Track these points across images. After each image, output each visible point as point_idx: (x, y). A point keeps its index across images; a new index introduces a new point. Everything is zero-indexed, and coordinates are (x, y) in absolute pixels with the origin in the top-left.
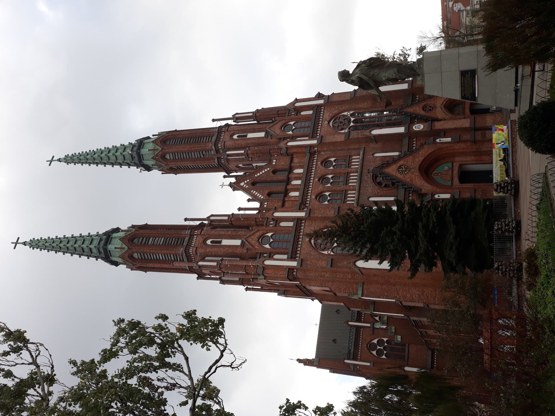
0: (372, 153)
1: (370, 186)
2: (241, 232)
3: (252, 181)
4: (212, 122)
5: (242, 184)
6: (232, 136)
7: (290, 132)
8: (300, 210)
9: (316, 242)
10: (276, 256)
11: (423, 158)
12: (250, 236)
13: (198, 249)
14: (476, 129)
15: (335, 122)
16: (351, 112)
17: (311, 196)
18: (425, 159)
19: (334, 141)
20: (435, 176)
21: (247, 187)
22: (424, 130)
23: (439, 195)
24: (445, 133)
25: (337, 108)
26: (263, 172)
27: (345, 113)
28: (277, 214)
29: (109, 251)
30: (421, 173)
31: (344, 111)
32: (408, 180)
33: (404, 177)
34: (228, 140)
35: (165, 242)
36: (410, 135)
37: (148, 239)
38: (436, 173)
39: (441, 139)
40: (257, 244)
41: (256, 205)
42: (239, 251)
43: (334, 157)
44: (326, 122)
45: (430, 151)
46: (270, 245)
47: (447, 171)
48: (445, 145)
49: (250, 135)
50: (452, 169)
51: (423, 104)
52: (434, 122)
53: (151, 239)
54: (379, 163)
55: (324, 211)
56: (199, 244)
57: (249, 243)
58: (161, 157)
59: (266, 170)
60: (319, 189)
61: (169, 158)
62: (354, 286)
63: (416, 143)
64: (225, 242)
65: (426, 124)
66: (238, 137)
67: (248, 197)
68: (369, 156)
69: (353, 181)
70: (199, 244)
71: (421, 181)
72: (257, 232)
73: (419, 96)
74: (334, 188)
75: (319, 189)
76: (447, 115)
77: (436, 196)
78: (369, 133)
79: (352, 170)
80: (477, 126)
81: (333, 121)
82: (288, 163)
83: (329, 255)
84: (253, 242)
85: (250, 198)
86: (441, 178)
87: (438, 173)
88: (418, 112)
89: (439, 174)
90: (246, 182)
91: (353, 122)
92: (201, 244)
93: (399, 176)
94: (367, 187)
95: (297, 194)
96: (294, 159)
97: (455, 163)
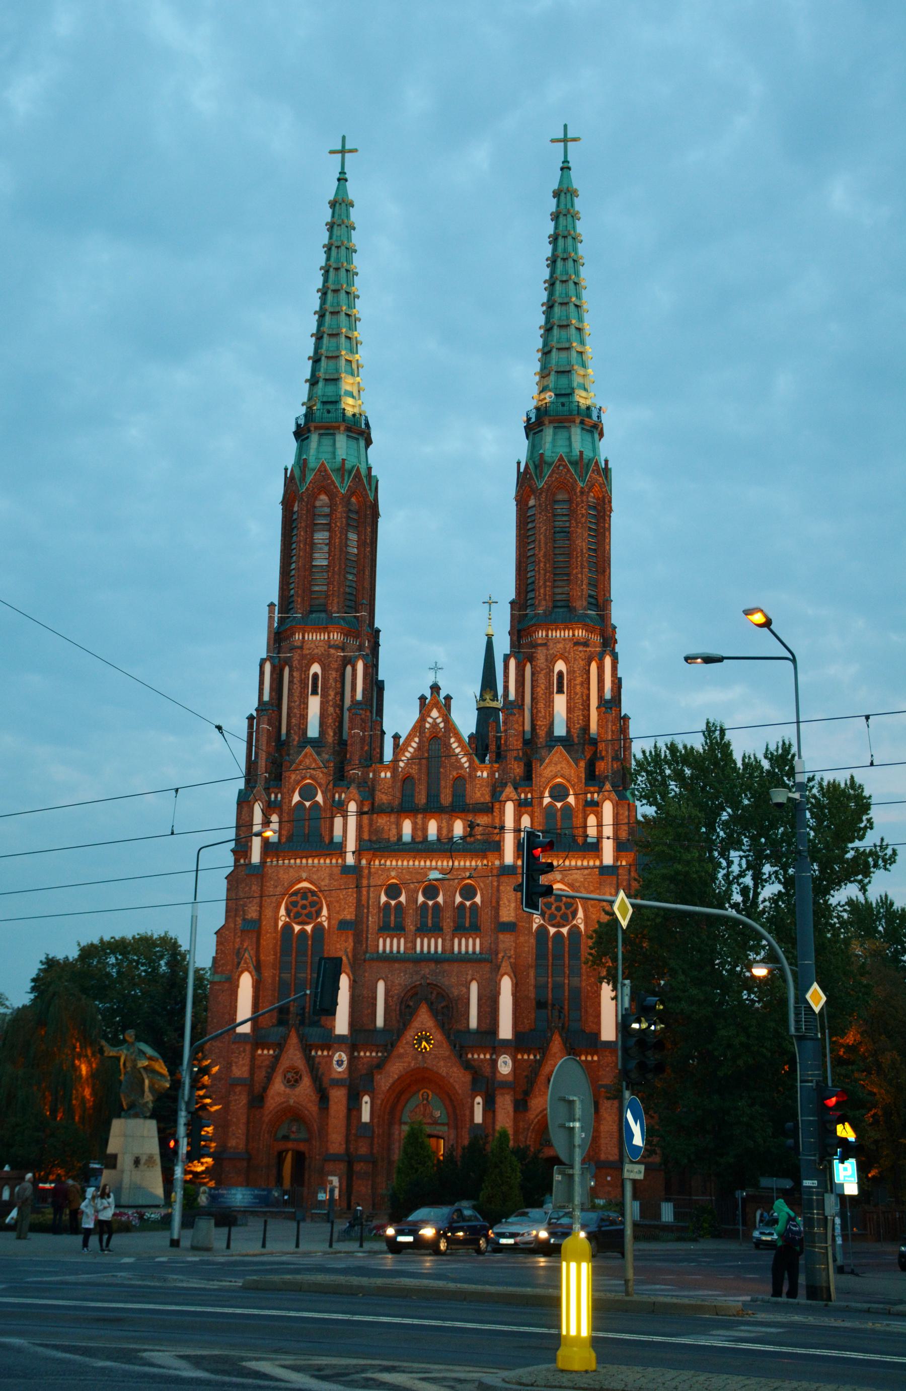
0: (478, 979)
1: (403, 979)
4: (419, 695)
5: (435, 713)
7: (547, 800)
11: (444, 1074)
13: (299, 652)
16: (582, 927)
19: (501, 902)
20: (423, 1095)
21: (427, 726)
22: (498, 1075)
23: (369, 1102)
27: (580, 914)
29: (307, 438)
31: (585, 911)
32: (402, 1051)
33: (407, 1043)
38: (428, 1096)
39: (481, 1106)
43: (482, 902)
45: (457, 1087)
46: (298, 803)
47: (432, 1116)
48: (468, 1113)
50: (435, 1123)
52: (512, 1093)
55: (350, 902)
56: (309, 649)
59: (464, 760)
62: (228, 967)
64: (314, 704)
65: (511, 1078)
67: (404, 735)
68: (470, 972)
70: (309, 649)
71: (397, 1072)
73: (595, 1061)
74: (411, 911)
76: (537, 1116)
77: (366, 1098)
78: (503, 971)
79: (448, 944)
83: (276, 919)
85: (402, 741)
86: (417, 1106)
87: (427, 1099)
88: (549, 1062)
89: (425, 1102)
91: (559, 934)
92: (310, 654)
94: (404, 975)
97: (446, 1128)
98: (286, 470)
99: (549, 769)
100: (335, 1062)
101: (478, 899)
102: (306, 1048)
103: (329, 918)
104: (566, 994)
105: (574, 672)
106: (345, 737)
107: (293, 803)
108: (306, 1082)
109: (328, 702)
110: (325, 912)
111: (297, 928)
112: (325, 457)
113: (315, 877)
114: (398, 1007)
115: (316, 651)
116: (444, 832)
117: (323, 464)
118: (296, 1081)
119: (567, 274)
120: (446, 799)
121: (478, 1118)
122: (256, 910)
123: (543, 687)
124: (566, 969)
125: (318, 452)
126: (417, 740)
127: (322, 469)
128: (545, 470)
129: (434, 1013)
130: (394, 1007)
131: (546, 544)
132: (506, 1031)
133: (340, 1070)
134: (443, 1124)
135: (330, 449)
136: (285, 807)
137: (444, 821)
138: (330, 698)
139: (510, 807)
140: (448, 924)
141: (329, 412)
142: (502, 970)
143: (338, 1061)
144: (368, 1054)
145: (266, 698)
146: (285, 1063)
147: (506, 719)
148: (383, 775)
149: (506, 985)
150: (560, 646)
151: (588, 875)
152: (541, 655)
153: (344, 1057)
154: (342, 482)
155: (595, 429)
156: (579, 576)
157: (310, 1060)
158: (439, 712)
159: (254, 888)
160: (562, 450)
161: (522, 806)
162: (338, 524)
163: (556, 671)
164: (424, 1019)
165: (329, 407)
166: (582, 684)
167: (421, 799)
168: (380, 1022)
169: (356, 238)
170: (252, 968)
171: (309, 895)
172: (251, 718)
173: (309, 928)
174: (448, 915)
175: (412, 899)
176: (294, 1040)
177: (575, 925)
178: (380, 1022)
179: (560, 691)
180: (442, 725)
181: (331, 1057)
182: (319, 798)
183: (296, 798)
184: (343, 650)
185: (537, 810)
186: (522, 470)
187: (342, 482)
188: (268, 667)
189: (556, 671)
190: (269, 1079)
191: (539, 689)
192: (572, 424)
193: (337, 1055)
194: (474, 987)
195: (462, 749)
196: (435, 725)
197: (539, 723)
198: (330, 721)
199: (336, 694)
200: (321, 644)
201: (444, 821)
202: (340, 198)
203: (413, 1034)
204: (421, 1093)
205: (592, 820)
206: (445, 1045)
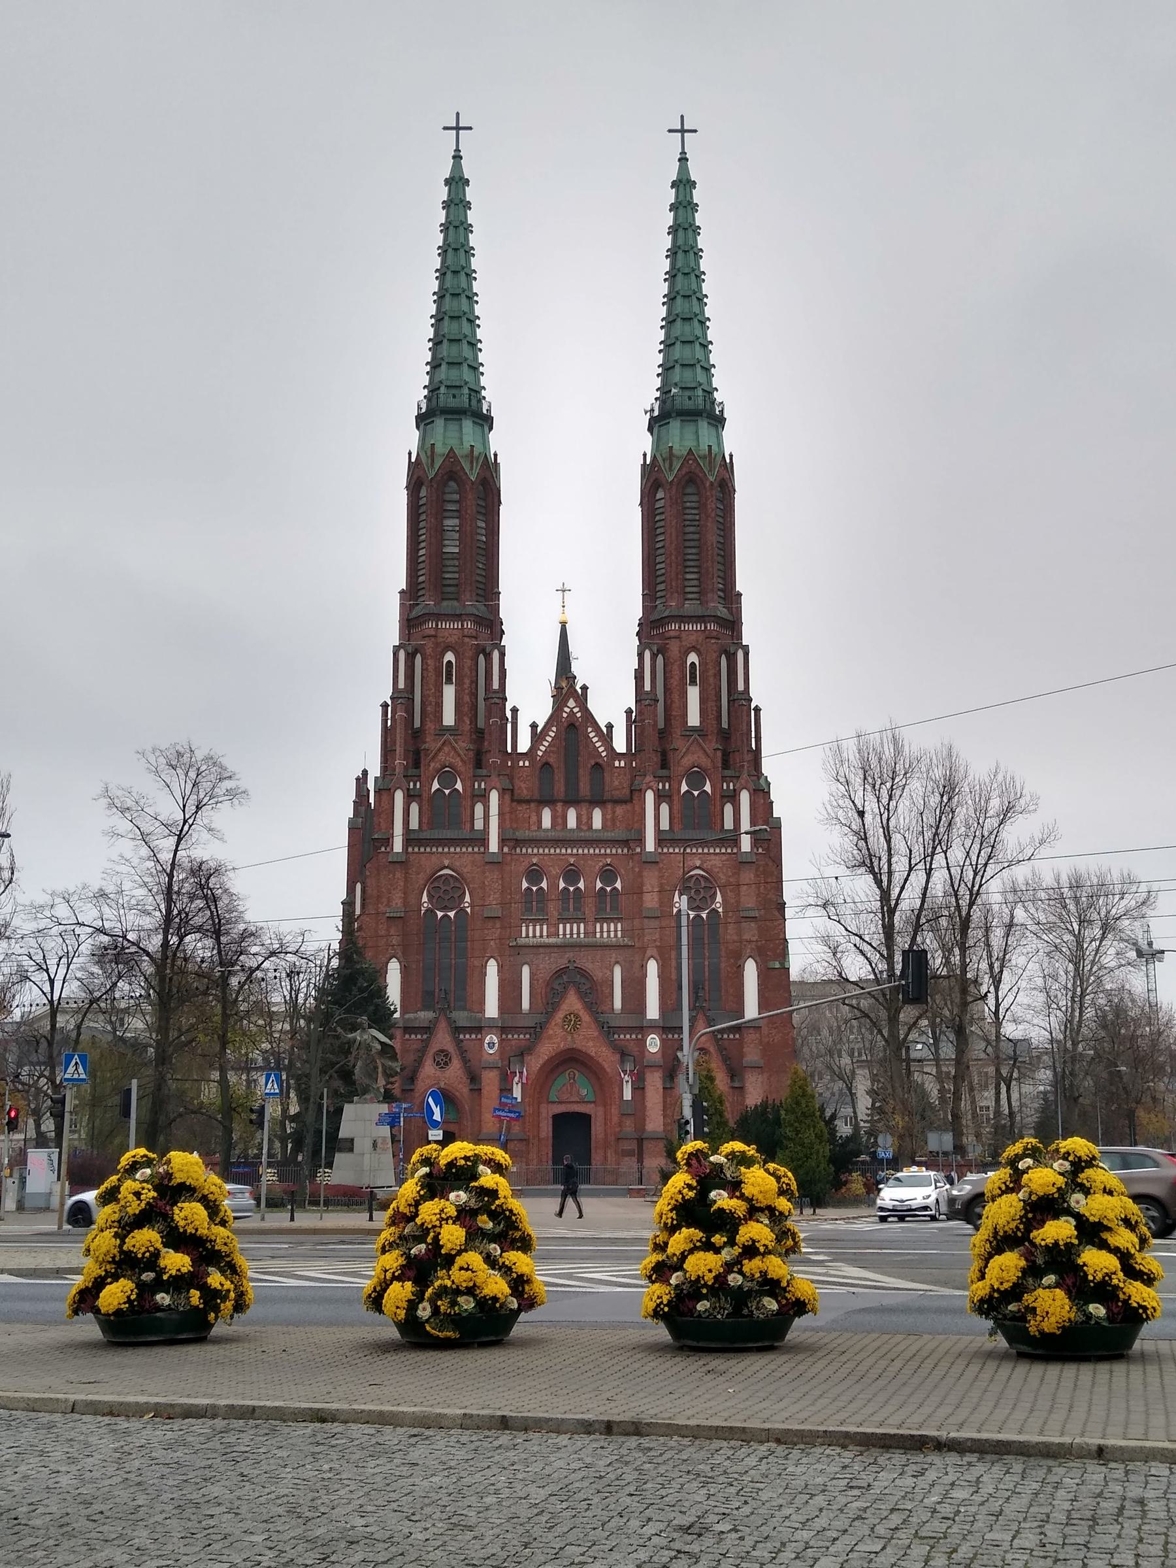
1: (550, 964)
2: (467, 726)
3: (577, 724)
5: (571, 703)
6: (694, 649)
7: (684, 788)
8: (503, 841)
9: (444, 878)
10: (414, 808)
11: (593, 1054)
12: (454, 748)
13: (433, 639)
14: (640, 1141)
15: (702, 880)
17: (535, 854)
18: (592, 1058)
21: (565, 715)
22: (647, 1053)
24: (639, 1089)
25: (731, 880)
26: (598, 745)
27: (719, 898)
28: (494, 796)
30: (562, 1052)
34: (684, 643)
35: (450, 556)
36: (644, 1028)
37: (455, 514)
40: (438, 766)
41: (524, 745)
42: (430, 726)
44: (698, 863)
45: (606, 1066)
51: (712, 1049)
53: (456, 522)
54: (598, 975)
57: (440, 750)
58: (656, 479)
60: (551, 868)
61: (657, 498)
63: (633, 1040)
64: (449, 693)
65: (659, 1056)
66: (693, 664)
72: (462, 760)
75: (551, 868)
79: (590, 929)
80: (645, 1142)
81: (702, 876)
82: (617, 794)
83: (421, 904)
84: (441, 757)
85: (539, 729)
90: (575, 710)
93: (560, 1015)
95: (547, 822)
96: (624, 806)
97: (593, 1105)
98: (410, 454)
99: (686, 759)
100: (486, 1045)
101: (618, 885)
102: (457, 1030)
103: (472, 905)
104: (707, 974)
105: (707, 664)
106: (481, 724)
107: (433, 790)
108: (456, 1063)
109: (463, 690)
110: (467, 898)
111: (440, 914)
112: (453, 442)
113: (458, 864)
114: (544, 991)
115: (449, 640)
116: (584, 820)
117: (451, 448)
118: (446, 1064)
119: (688, 266)
120: (585, 789)
121: (628, 1095)
122: (400, 898)
123: (677, 678)
124: (706, 951)
125: (681, 439)
126: (554, 729)
127: (451, 455)
128: (675, 463)
129: (582, 995)
130: (539, 991)
131: (677, 536)
133: (491, 1052)
134: (591, 1102)
135: (457, 435)
136: (425, 795)
137: (584, 809)
138: (466, 686)
139: (650, 796)
141: (454, 396)
142: (649, 953)
143: (489, 1044)
144: (516, 1036)
145: (401, 685)
146: (434, 1047)
147: (640, 712)
148: (521, 764)
149: (652, 967)
150: (693, 638)
151: (727, 860)
152: (674, 648)
153: (495, 1040)
154: (472, 469)
155: (719, 421)
156: (711, 569)
157: (458, 1043)
158: (575, 701)
159: (398, 875)
160: (690, 443)
162: (469, 512)
163: (688, 664)
164: (572, 1002)
165: (454, 391)
166: (715, 675)
168: (526, 1005)
169: (472, 217)
170: (400, 954)
171: (452, 881)
172: (385, 706)
173: (452, 914)
175: (553, 885)
176: (443, 1025)
177: (714, 909)
178: (526, 1005)
179: (693, 682)
180: (579, 715)
181: (482, 1041)
182: (459, 786)
183: (436, 786)
184: (476, 638)
185: (676, 798)
186: (648, 462)
187: (472, 469)
188: (402, 655)
189: (688, 664)
190: (419, 1062)
191: (672, 681)
192: (699, 418)
193: (488, 1038)
194: (618, 972)
195: (600, 738)
196: (571, 713)
197: (674, 713)
198: (466, 709)
199: (472, 682)
200: (455, 632)
201: (584, 809)
202: (457, 176)
203: (562, 1016)
204: (568, 1072)
205: (728, 809)
206: (593, 1026)
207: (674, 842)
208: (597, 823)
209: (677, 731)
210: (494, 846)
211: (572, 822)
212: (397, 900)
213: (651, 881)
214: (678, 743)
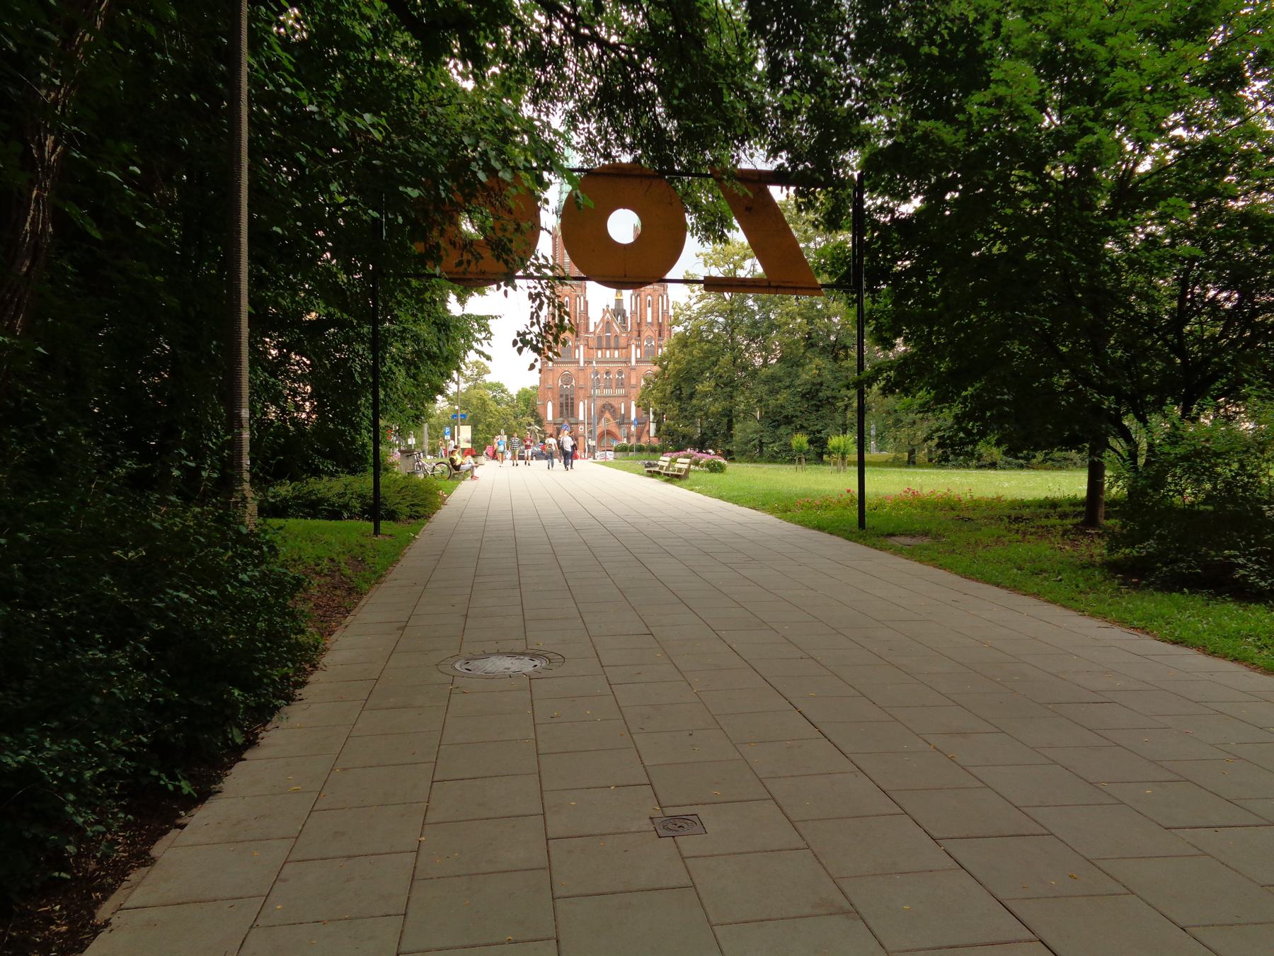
1: (600, 402)
8: (585, 362)
28: (582, 347)
49: (649, 310)
54: (616, 406)
69: (606, 392)
120: (613, 345)
129: (610, 413)
132: (633, 417)
139: (633, 347)
140: (614, 385)
161: (637, 346)
164: (607, 415)
167: (604, 344)
174: (614, 382)
176: (566, 423)
207: (642, 362)
208: (616, 356)
209: (643, 324)
210: (582, 364)
211: (608, 356)
212: (550, 382)
213: (633, 374)
214: (644, 328)
